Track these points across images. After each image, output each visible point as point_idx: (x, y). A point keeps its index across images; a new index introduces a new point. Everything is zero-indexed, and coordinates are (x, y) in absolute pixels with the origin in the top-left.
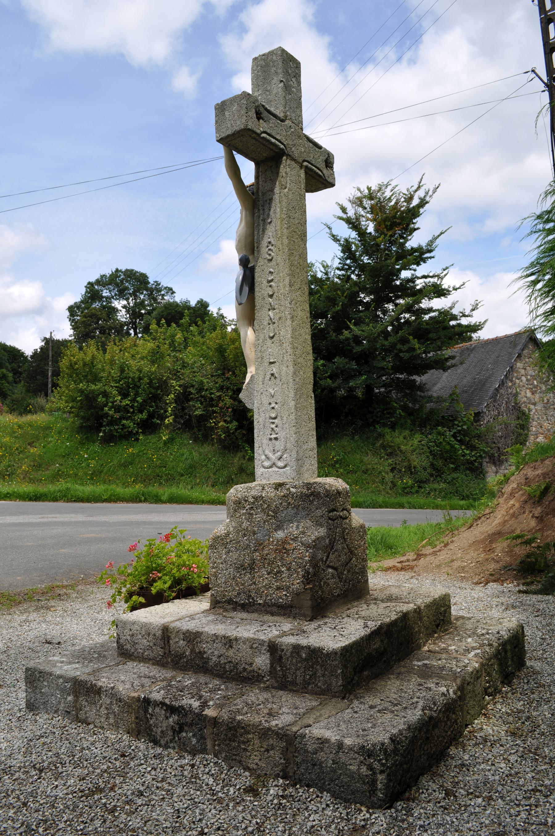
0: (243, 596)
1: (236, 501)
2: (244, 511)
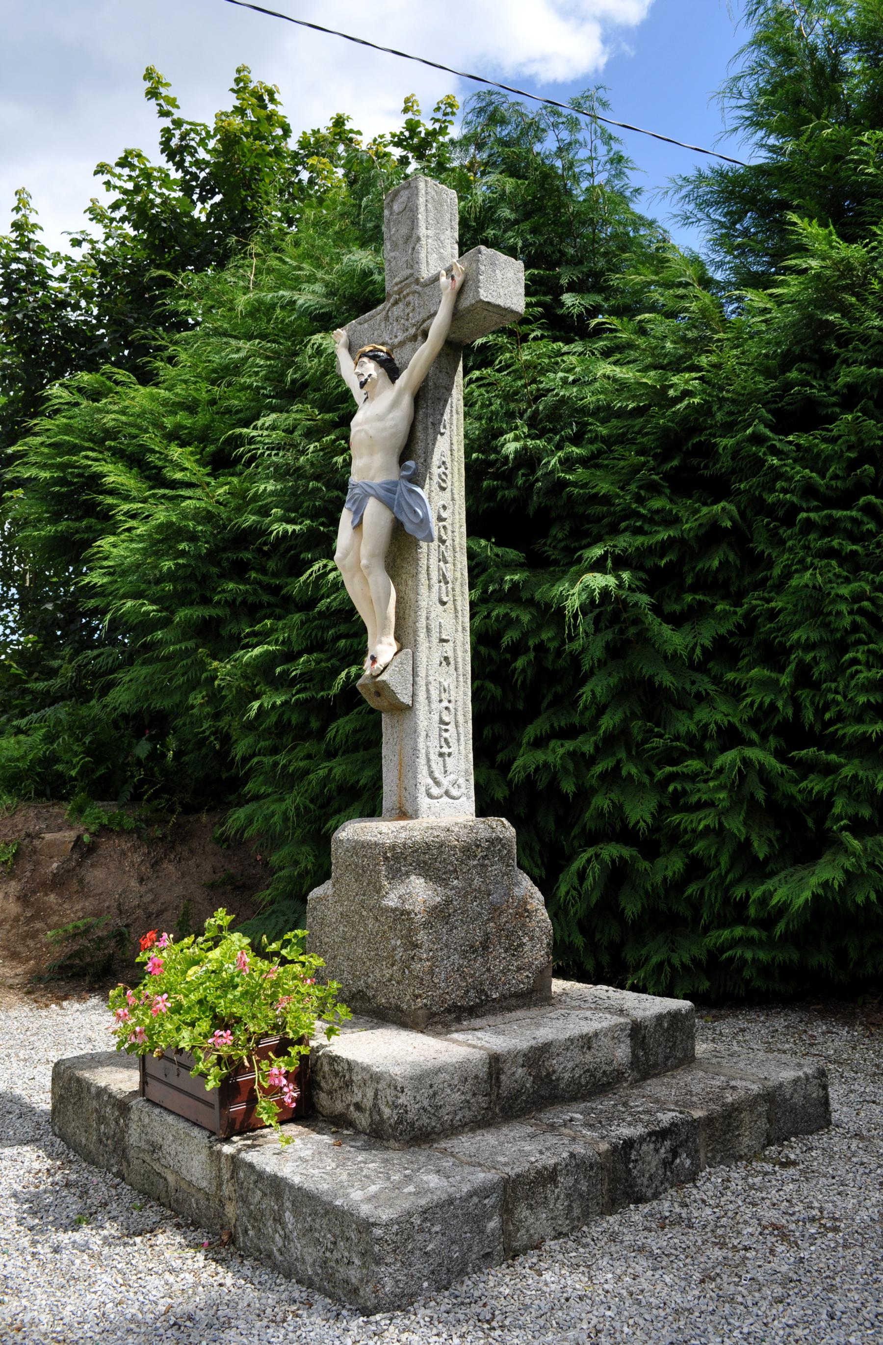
0: (472, 993)
1: (464, 847)
2: (476, 862)
